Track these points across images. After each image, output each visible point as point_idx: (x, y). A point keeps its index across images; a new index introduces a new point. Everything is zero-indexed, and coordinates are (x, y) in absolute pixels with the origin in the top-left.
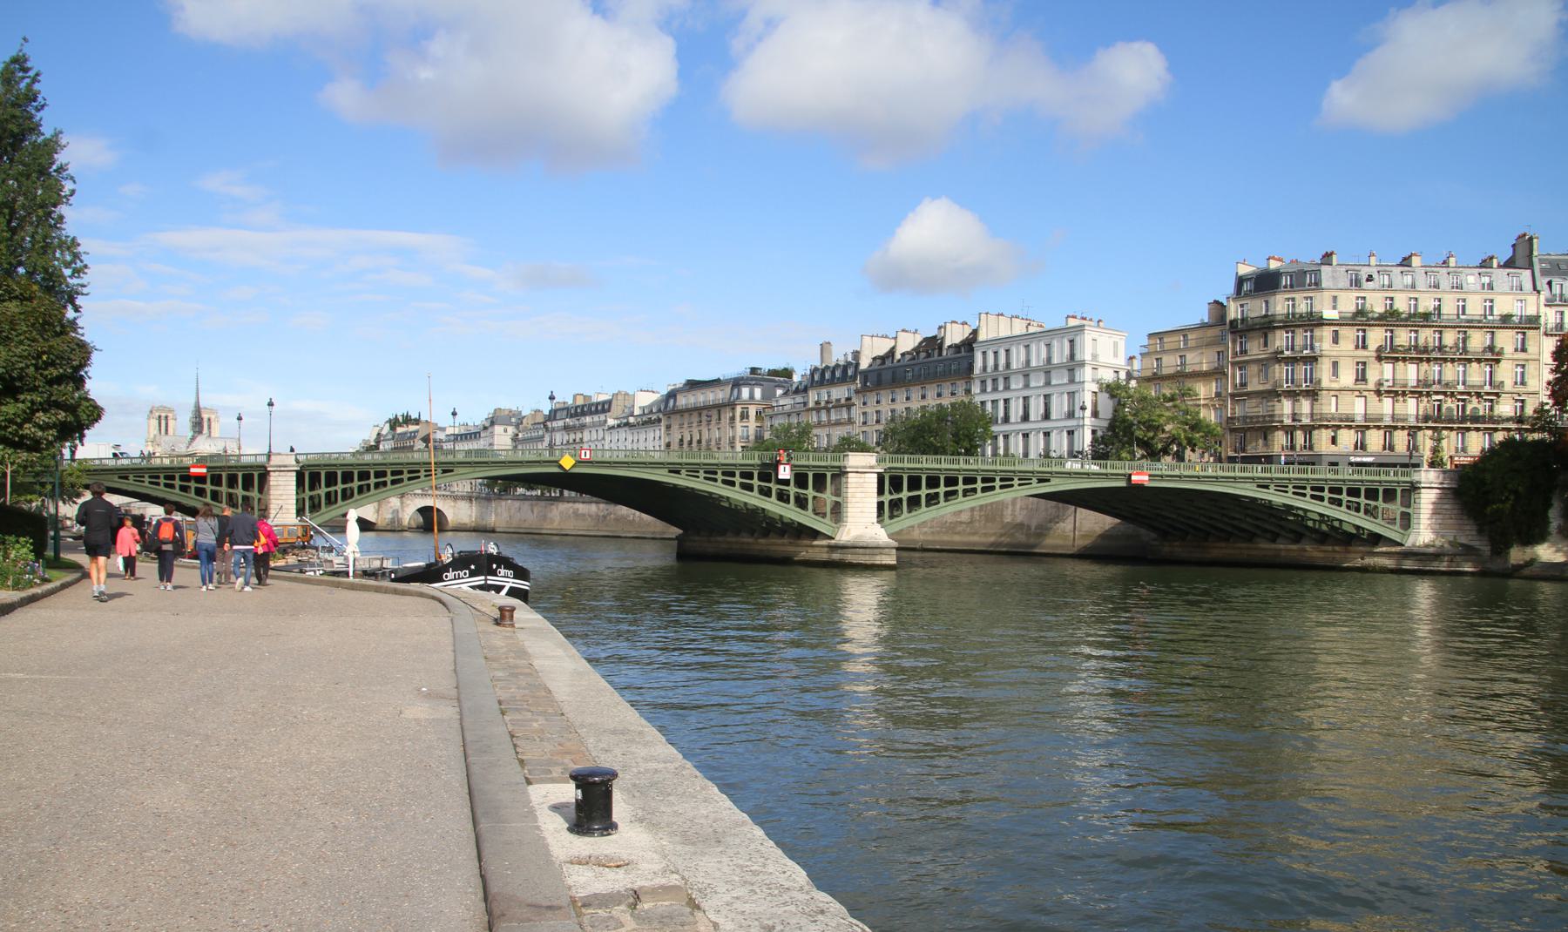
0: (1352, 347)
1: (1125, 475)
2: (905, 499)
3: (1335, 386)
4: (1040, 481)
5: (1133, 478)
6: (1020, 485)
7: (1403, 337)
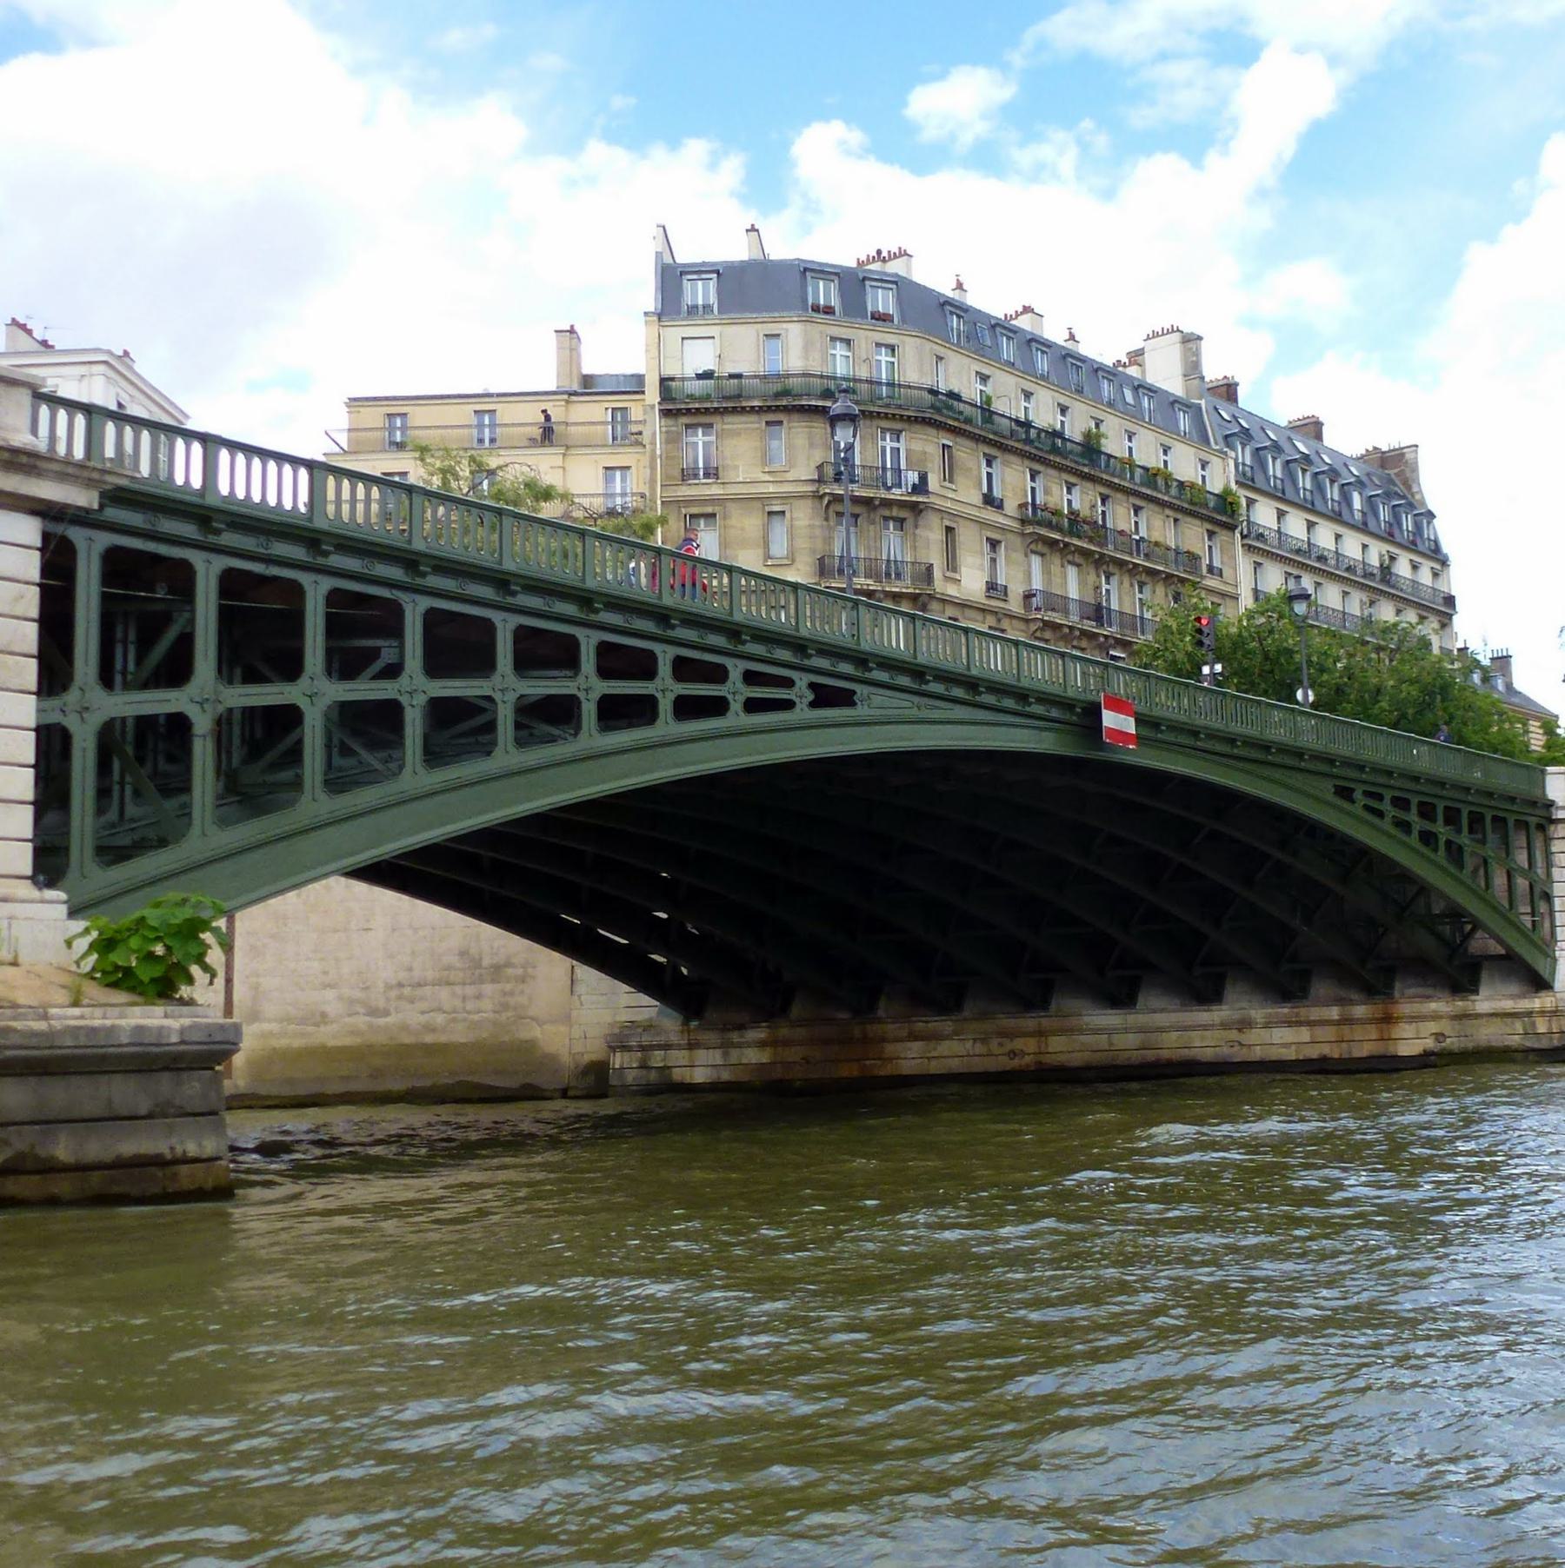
0: (977, 499)
1: (1066, 704)
2: (202, 724)
3: (951, 590)
4: (825, 697)
5: (1110, 719)
6: (752, 706)
7: (1060, 495)
